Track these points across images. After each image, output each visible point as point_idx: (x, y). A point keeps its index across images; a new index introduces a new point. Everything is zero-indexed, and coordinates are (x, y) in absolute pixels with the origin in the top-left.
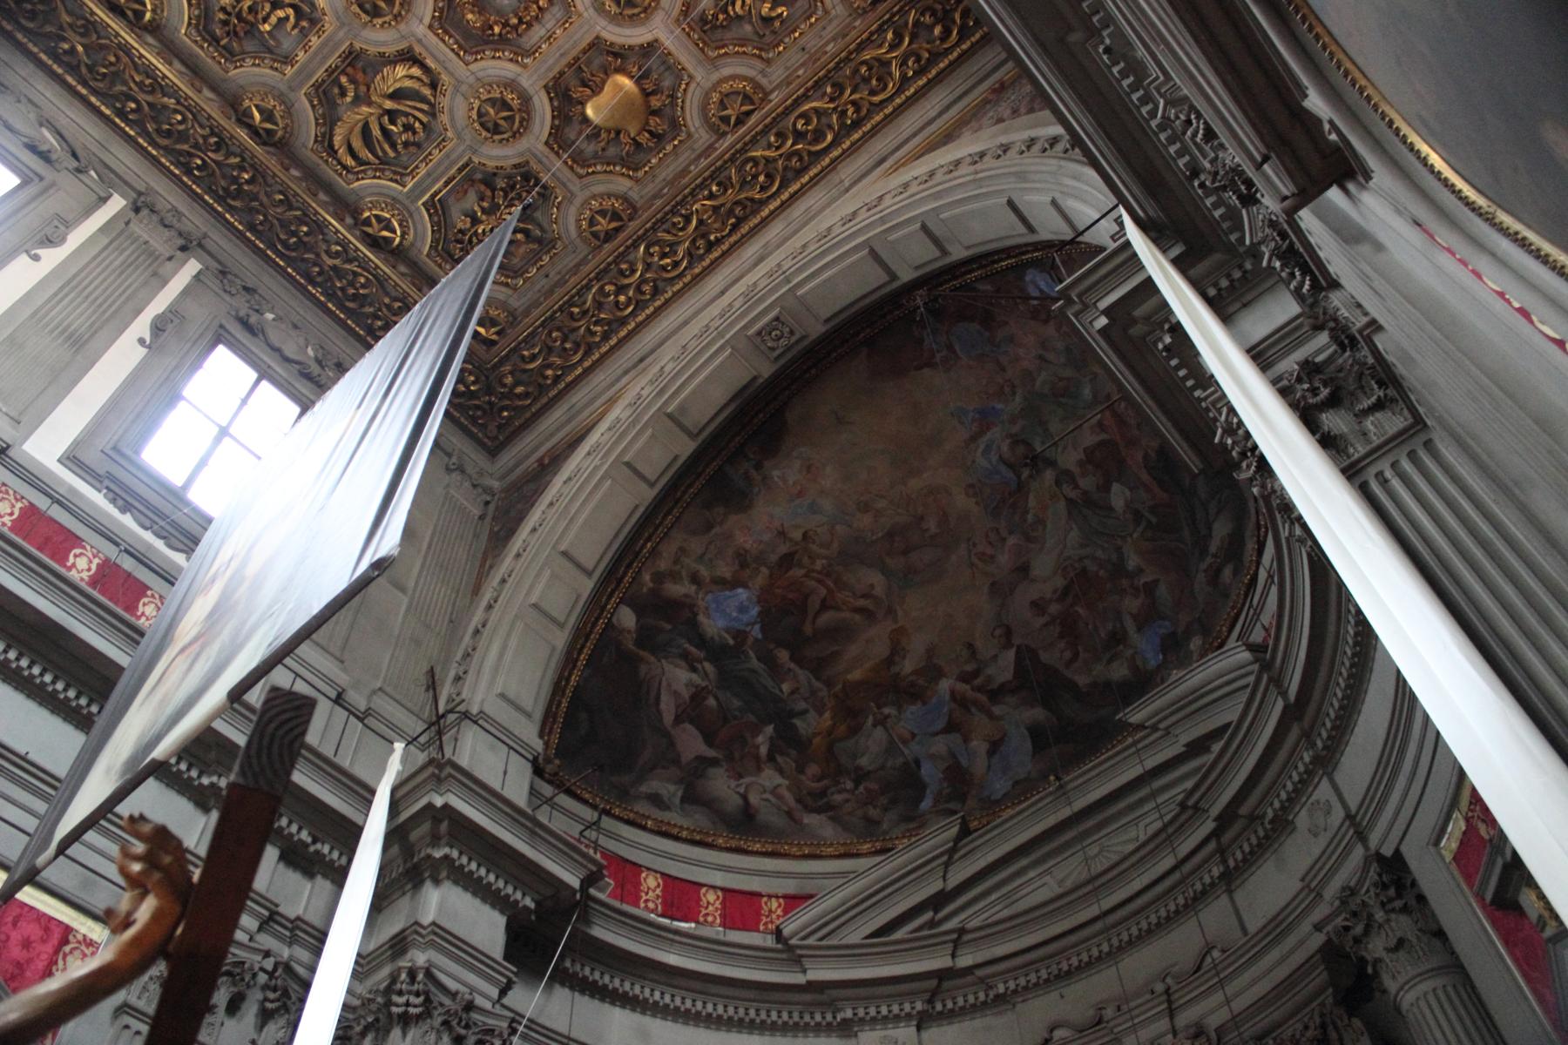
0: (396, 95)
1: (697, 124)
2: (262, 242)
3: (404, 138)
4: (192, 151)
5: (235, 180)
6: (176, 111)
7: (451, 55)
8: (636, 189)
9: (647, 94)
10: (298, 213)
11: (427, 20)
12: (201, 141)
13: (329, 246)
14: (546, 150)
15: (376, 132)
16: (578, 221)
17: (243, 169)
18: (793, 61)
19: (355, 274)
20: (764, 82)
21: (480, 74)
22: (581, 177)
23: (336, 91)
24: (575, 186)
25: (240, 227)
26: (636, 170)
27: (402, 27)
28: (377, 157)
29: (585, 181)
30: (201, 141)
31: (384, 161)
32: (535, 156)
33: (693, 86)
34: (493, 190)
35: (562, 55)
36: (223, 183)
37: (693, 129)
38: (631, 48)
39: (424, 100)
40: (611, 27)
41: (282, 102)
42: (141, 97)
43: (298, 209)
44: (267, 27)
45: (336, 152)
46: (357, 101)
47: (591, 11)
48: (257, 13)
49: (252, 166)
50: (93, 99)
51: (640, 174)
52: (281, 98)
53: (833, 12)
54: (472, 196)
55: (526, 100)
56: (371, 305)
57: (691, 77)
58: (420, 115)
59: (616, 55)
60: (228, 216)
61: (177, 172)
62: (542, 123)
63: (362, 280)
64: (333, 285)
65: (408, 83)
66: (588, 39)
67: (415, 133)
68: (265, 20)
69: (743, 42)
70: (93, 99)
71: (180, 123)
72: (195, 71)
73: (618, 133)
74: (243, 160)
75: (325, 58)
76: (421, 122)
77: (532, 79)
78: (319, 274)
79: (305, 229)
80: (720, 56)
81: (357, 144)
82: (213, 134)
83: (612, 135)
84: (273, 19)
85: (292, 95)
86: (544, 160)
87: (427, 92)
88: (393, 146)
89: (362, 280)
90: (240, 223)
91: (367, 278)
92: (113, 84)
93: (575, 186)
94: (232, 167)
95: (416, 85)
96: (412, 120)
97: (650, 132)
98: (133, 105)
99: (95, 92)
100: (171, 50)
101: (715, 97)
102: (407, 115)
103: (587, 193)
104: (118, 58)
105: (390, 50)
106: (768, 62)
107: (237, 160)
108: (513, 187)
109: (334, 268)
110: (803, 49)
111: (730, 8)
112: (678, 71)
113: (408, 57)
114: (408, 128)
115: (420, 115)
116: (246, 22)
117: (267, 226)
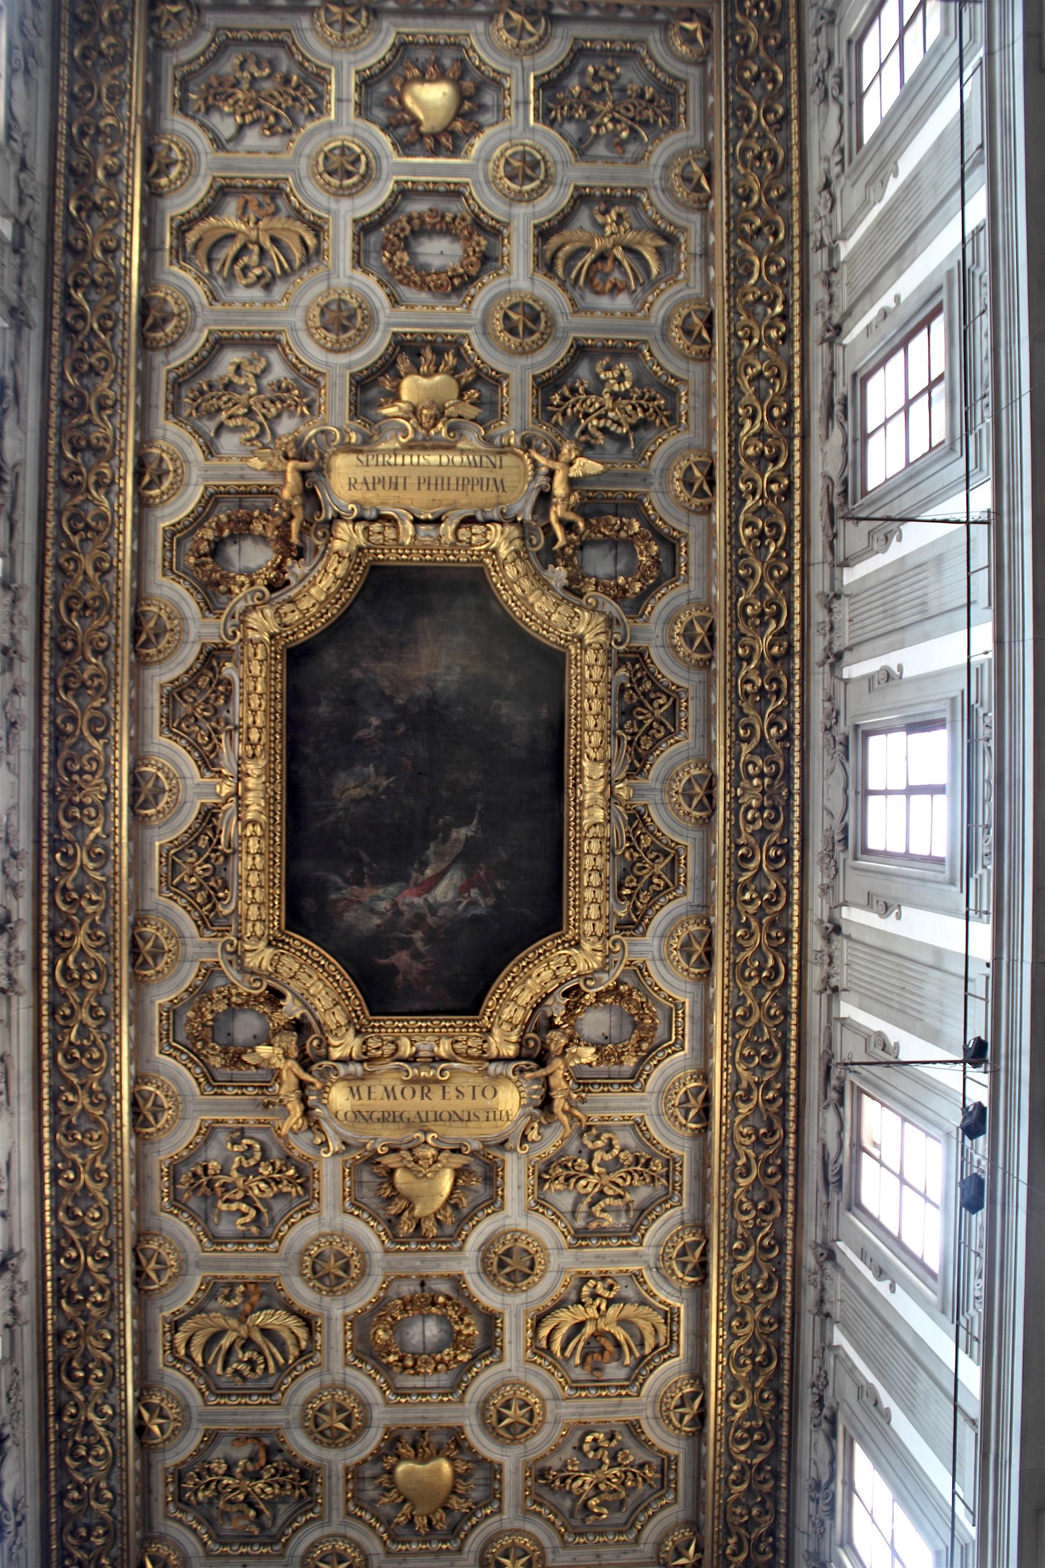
0: (265, 1332)
1: (474, 1548)
2: (54, 1352)
3: (242, 1367)
4: (78, 1245)
5: (87, 1294)
6: (99, 1209)
7: (341, 1348)
8: (382, 1557)
9: (454, 1491)
10: (109, 1359)
11: (349, 1310)
12: (94, 1244)
13: (104, 1404)
14: (342, 1473)
15: (225, 1342)
16: (313, 1546)
17: (101, 1290)
18: (583, 1558)
19: (100, 1442)
20: (550, 1556)
21: (349, 1380)
22: (348, 1514)
23: (226, 1291)
24: (338, 1516)
25: (50, 1328)
26: (394, 1541)
27: (327, 1300)
28: (204, 1361)
29: (348, 1520)
30: (94, 1244)
31: (205, 1370)
32: (330, 1471)
33: (496, 1518)
34: (268, 1462)
35: (424, 1418)
36: (74, 1287)
37: (466, 1549)
38: (470, 1448)
39: (284, 1353)
40: (477, 1429)
41: (180, 1267)
42: (84, 1176)
43: (111, 1355)
44: (224, 1207)
45: (177, 1331)
46: (233, 1311)
47: (474, 1406)
48: (227, 1191)
49: (112, 1295)
50: (47, 1147)
51: (394, 1547)
52: (183, 1262)
53: (642, 1547)
54: (246, 1450)
55: (366, 1424)
56: (85, 1474)
57: (500, 1510)
58: (271, 1363)
59: (458, 1445)
60: (49, 1311)
61: (48, 1247)
62: (360, 1452)
63: (102, 1451)
64: (74, 1434)
65: (285, 1334)
66: (453, 1422)
67: (253, 1370)
68: (227, 1201)
69: (556, 1511)
70: (47, 1147)
71: (94, 1219)
72: (140, 1188)
73: (405, 1501)
74: (110, 1285)
75: (247, 1268)
76: (266, 1368)
77: (382, 1417)
78: (72, 1416)
79: (100, 1374)
80: (534, 1512)
81: (199, 1341)
82: (108, 1249)
83: (399, 1500)
84: (234, 1207)
85: (192, 1269)
86: (334, 1479)
87: (293, 1352)
88: (225, 1365)
89: (102, 1451)
90: (53, 1324)
91: (107, 1452)
92: (73, 1149)
93: (338, 1516)
94: (94, 1282)
95: (290, 1342)
96: (261, 1360)
97: (430, 1521)
98: (72, 1176)
99: (54, 1142)
100: (139, 1161)
101: (507, 1541)
102: (261, 1353)
103: (341, 1530)
104: (100, 1137)
105: (300, 1304)
106: (565, 1544)
107: (107, 1281)
108: (285, 1474)
109: (88, 1423)
110: (598, 1556)
111: (569, 1481)
112: (494, 1496)
113: (308, 1322)
114: (251, 1362)
115: (271, 1363)
116: (213, 1189)
117: (71, 1345)
